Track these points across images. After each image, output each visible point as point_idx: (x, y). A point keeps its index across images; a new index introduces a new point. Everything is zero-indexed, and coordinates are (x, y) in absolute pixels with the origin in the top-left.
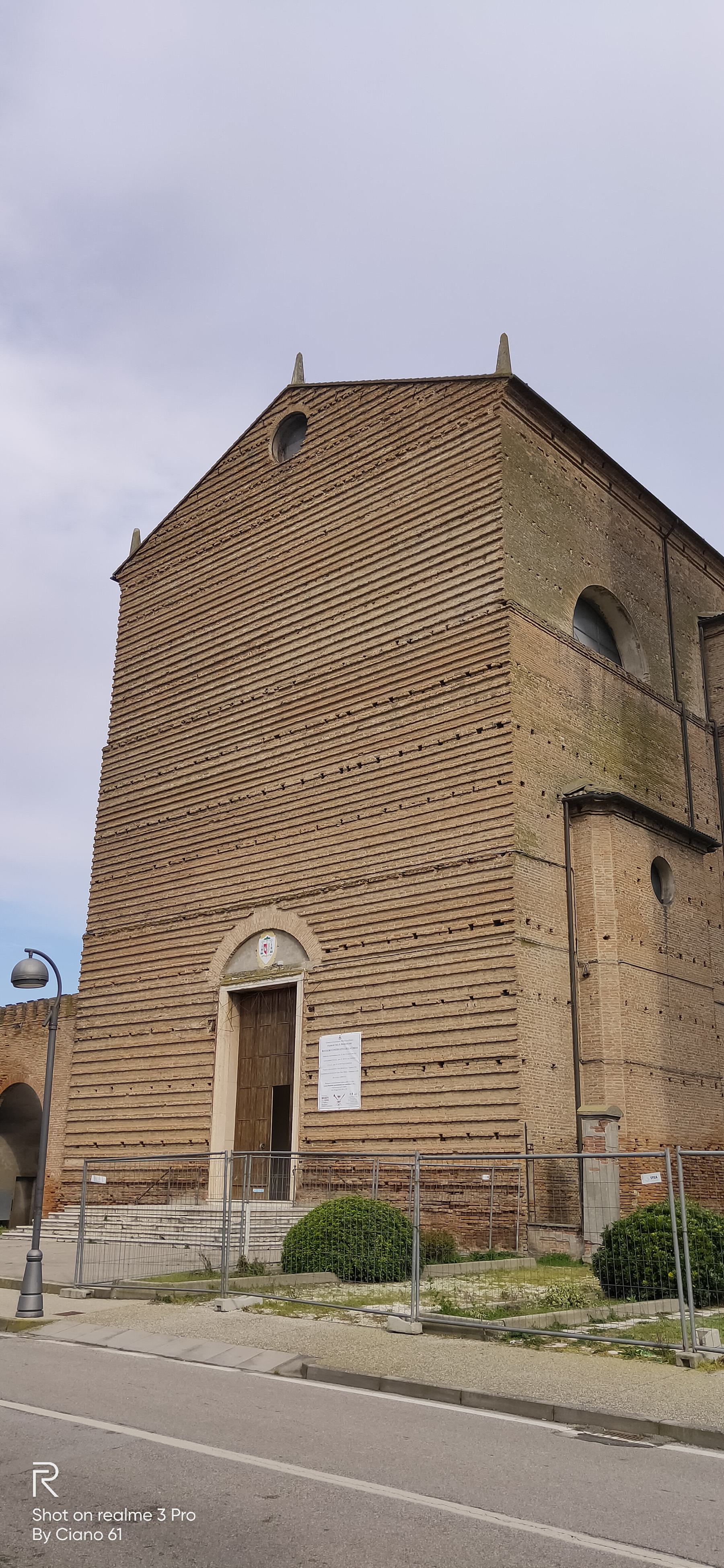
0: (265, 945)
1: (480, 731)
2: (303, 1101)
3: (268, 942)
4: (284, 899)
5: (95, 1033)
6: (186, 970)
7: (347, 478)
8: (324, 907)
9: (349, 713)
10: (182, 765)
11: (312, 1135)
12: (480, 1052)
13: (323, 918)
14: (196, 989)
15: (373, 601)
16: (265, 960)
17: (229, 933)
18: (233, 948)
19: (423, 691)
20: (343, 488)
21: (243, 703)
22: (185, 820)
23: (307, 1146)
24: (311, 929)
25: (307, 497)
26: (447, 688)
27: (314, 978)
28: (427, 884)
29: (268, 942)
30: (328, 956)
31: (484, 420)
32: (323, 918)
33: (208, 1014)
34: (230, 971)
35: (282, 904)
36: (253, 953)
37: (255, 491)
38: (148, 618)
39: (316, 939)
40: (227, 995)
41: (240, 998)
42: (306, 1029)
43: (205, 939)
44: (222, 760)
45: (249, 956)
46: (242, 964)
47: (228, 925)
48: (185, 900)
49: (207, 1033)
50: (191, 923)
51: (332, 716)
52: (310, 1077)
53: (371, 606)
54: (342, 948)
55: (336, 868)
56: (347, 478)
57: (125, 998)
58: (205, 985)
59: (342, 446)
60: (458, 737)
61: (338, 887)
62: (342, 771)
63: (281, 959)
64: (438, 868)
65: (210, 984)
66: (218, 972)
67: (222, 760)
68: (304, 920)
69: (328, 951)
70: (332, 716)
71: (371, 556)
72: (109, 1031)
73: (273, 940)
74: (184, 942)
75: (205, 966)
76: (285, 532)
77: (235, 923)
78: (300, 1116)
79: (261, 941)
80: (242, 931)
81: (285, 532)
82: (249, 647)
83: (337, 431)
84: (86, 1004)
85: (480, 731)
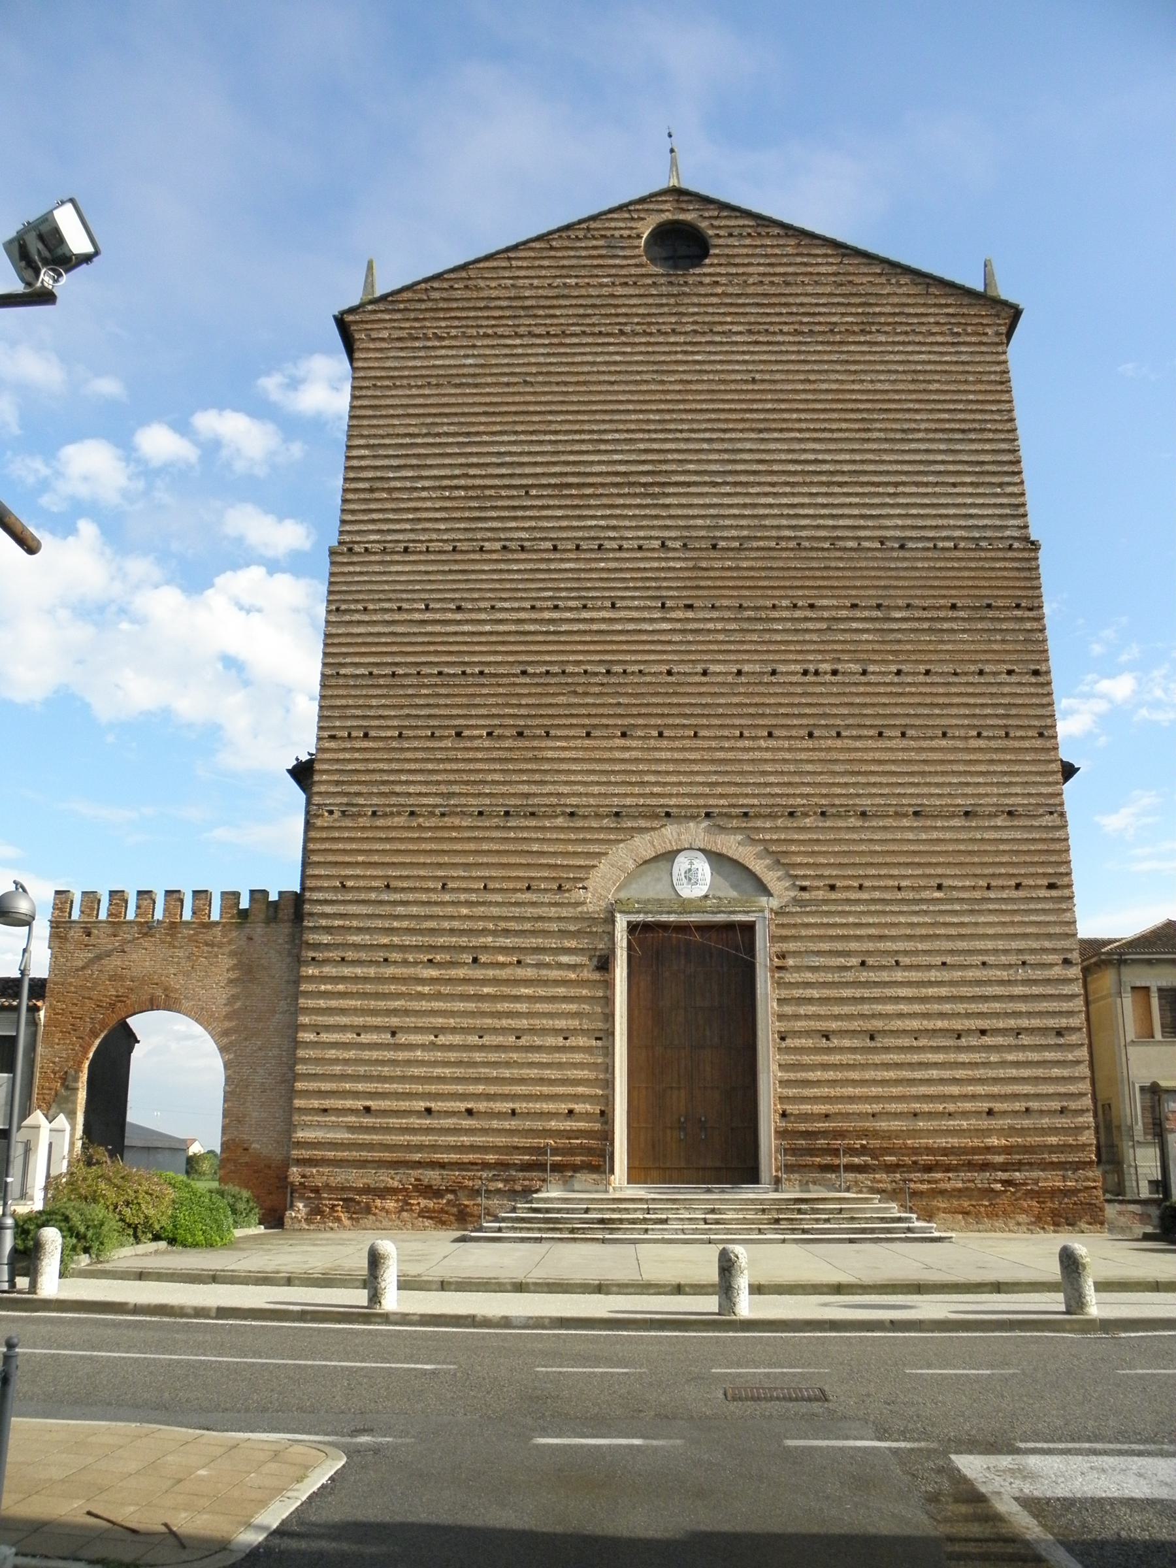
1: (1010, 672)
5: (350, 955)
7: (785, 328)
9: (812, 606)
10: (507, 605)
11: (790, 1108)
12: (1036, 1022)
15: (840, 484)
19: (924, 609)
20: (780, 338)
21: (620, 548)
22: (517, 680)
25: (719, 328)
26: (955, 614)
28: (951, 831)
30: (806, 895)
31: (984, 339)
37: (620, 291)
38: (414, 391)
40: (625, 925)
44: (585, 615)
46: (649, 888)
48: (525, 789)
51: (785, 603)
53: (837, 490)
55: (808, 790)
56: (785, 328)
57: (414, 910)
59: (773, 290)
60: (981, 673)
62: (805, 673)
64: (967, 814)
67: (585, 615)
69: (803, 889)
70: (785, 603)
71: (831, 431)
72: (379, 956)
76: (680, 357)
80: (644, 846)
81: (680, 357)
82: (627, 481)
83: (762, 269)
84: (328, 909)
85: (1010, 672)
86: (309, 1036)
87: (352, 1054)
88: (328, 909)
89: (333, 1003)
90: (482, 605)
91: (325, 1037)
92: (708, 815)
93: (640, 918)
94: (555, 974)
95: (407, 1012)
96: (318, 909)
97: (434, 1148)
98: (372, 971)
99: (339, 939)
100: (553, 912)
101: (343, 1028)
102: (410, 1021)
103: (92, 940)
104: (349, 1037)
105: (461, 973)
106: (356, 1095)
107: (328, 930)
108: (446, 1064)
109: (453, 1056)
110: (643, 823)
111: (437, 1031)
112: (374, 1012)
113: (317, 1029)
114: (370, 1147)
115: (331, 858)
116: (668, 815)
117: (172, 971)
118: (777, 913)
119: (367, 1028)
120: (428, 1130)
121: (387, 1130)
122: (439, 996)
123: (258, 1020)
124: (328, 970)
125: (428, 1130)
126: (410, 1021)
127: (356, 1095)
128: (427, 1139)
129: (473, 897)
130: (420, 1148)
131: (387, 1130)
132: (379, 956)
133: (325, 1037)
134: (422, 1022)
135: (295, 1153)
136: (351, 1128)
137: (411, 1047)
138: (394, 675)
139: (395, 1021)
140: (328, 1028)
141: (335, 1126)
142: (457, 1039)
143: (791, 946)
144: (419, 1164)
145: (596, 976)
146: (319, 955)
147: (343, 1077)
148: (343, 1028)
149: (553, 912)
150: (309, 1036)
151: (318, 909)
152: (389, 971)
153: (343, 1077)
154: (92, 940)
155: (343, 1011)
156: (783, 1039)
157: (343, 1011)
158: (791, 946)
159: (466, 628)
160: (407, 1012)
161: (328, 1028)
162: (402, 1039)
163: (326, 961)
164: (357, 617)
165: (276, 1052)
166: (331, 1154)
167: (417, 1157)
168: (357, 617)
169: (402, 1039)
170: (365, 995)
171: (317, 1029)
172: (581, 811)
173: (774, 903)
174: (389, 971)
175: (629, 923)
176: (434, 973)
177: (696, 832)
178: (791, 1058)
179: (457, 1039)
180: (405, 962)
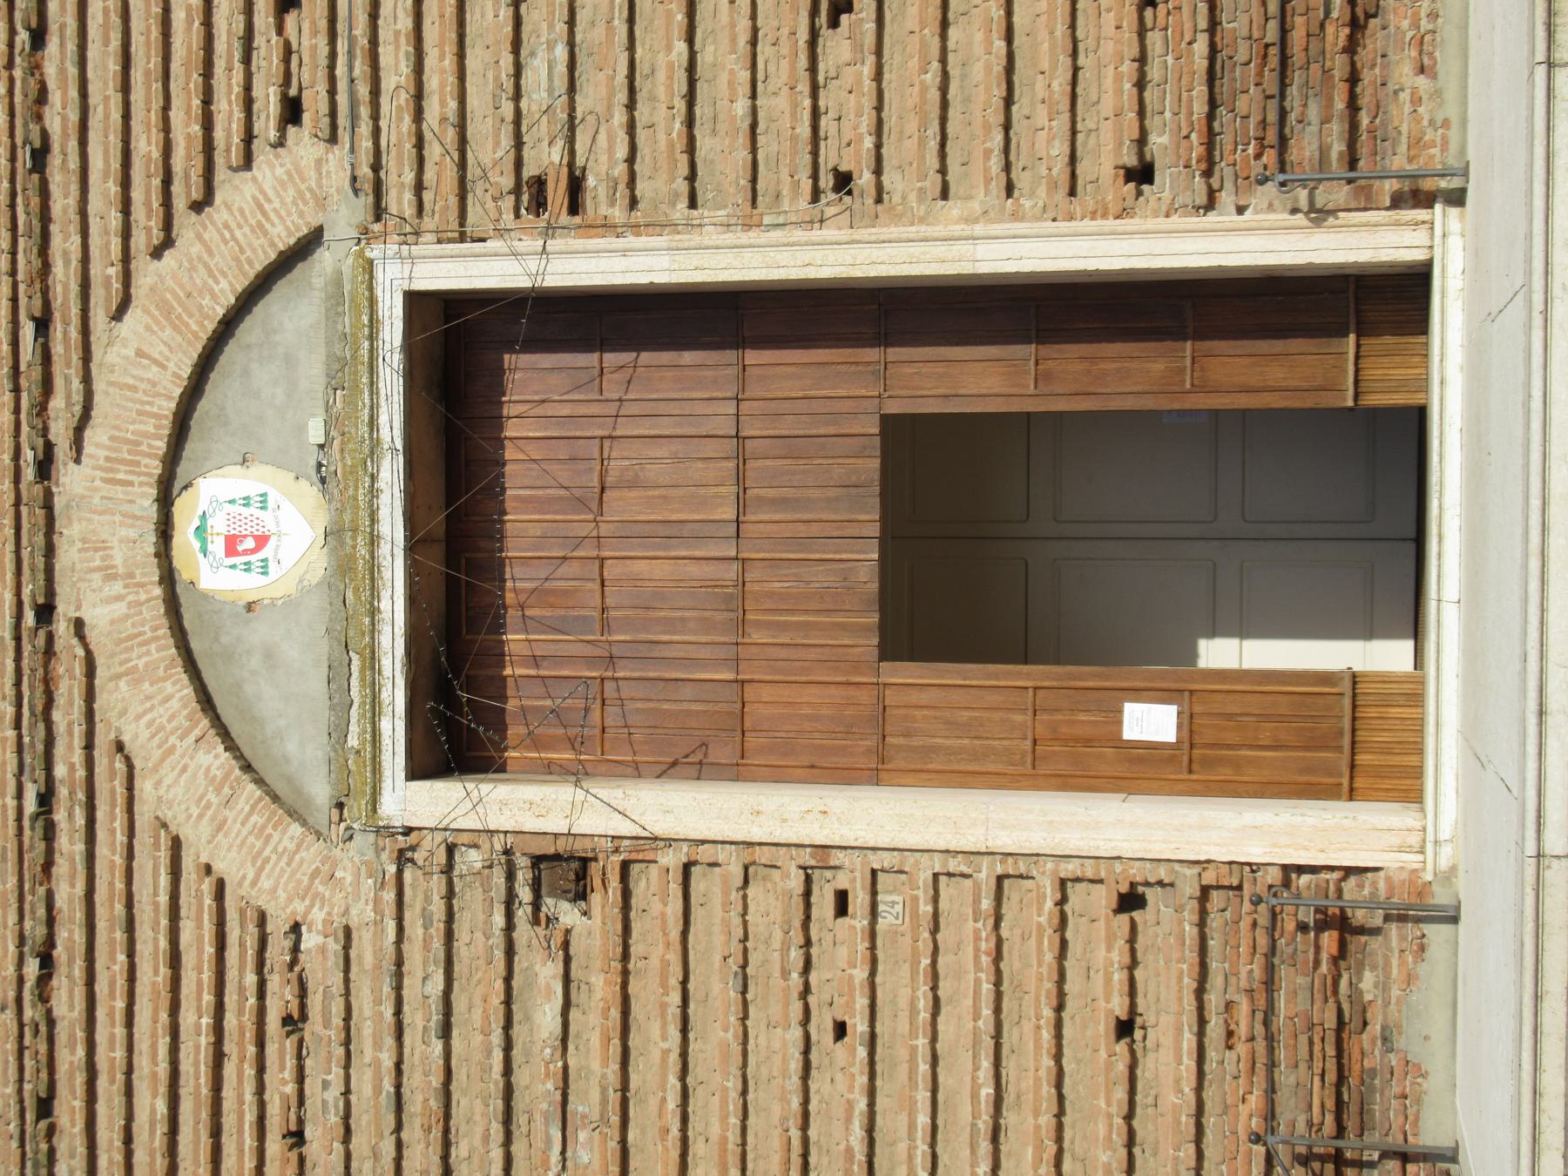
0: (231, 550)
2: (954, 208)
3: (219, 526)
4: (42, 408)
6: (280, 1083)
8: (103, 159)
11: (1106, 154)
13: (146, 146)
14: (372, 1008)
16: (296, 530)
17: (145, 787)
18: (216, 758)
23: (1164, 176)
24: (184, 220)
27: (399, 200)
29: (219, 526)
30: (315, 104)
32: (146, 146)
33: (499, 920)
34: (320, 792)
35: (60, 432)
36: (259, 632)
39: (234, 191)
41: (457, 727)
42: (618, 214)
43: (152, 941)
45: (269, 655)
47: (109, 787)
49: (588, 924)
50: (70, 1058)
52: (843, 181)
54: (290, 19)
58: (366, 952)
61: (35, 68)
63: (302, 429)
65: (361, 914)
66: (313, 852)
68: (147, 274)
69: (292, 111)
73: (213, 495)
74: (151, 1105)
75: (278, 952)
77: (103, 740)
78: (1016, 216)
79: (211, 574)
80: (144, 705)
92: (45, 467)
93: (394, 730)
94: (593, 1062)
100: (374, 1053)
110: (67, 715)
116: (46, 612)
118: (379, 212)
143: (490, 148)
145: (604, 901)
149: (374, 1053)
156: (843, 181)
158: (490, 148)
172: (35, 930)
173: (344, 217)
175: (418, 770)
177: (100, 504)
178: (909, 146)
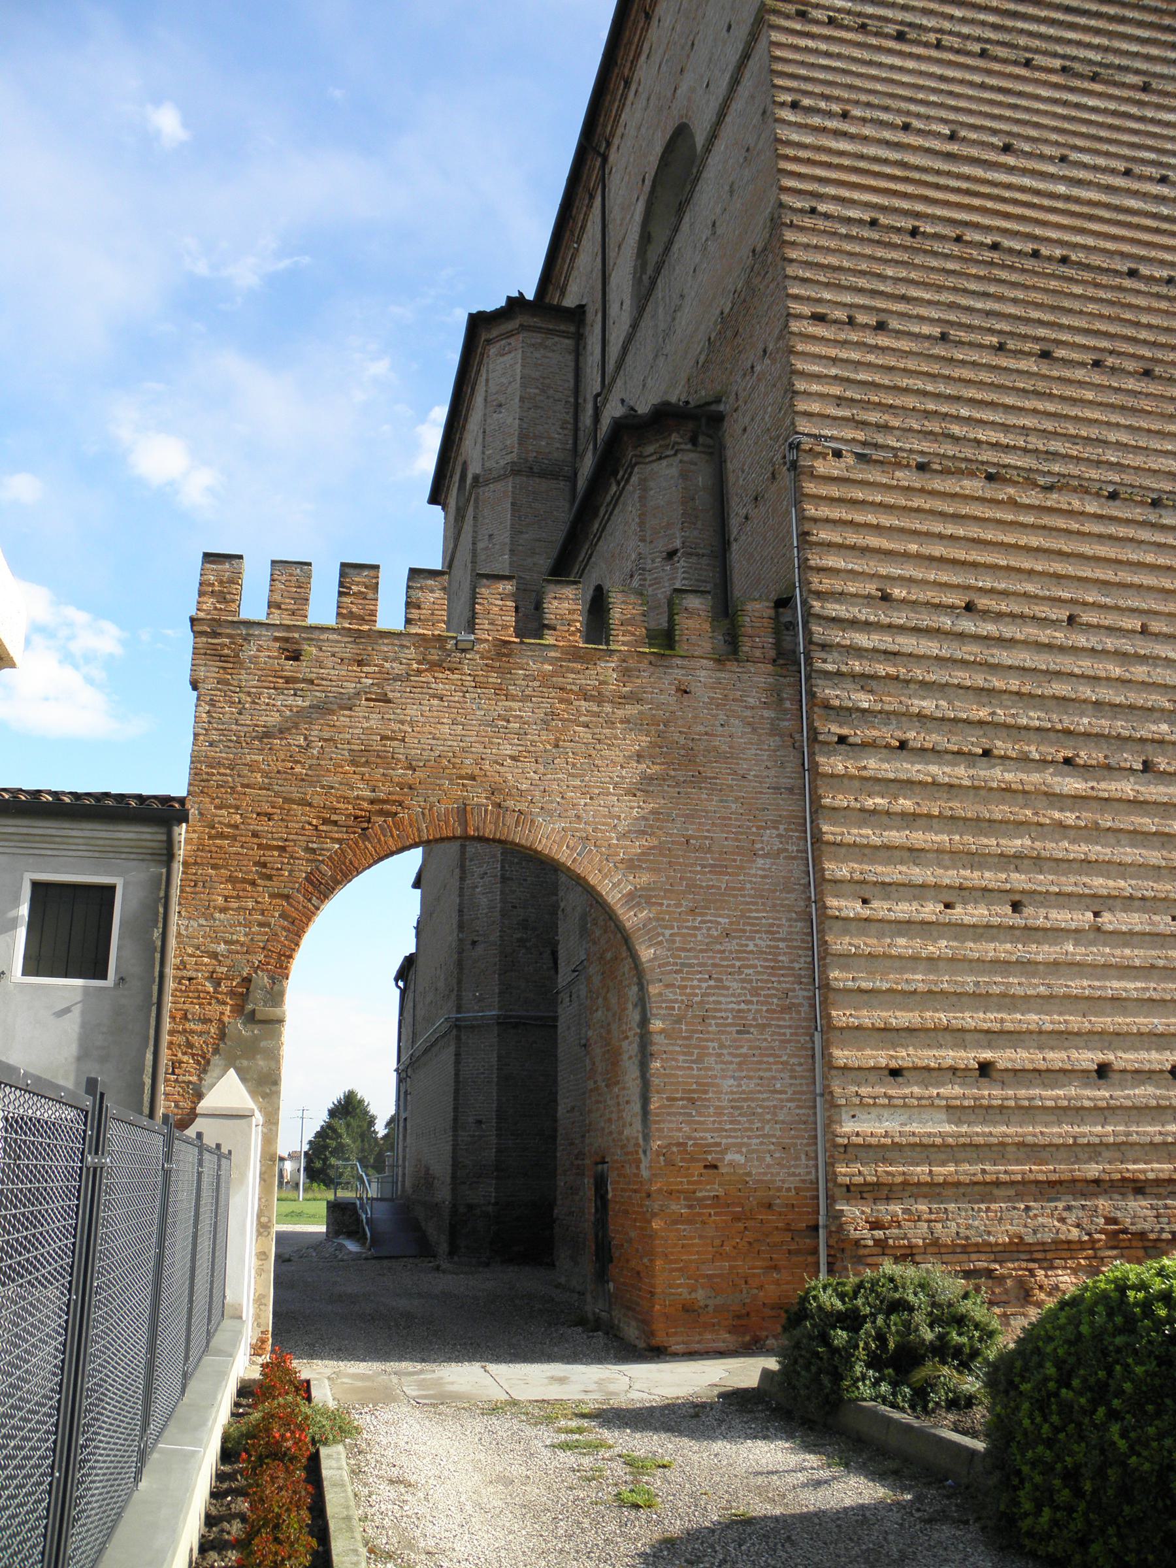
84: (863, 640)
86: (852, 908)
87: (941, 947)
88: (863, 640)
89: (895, 836)
90: (1048, 150)
91: (880, 908)
95: (1038, 862)
96: (837, 636)
97: (1122, 1149)
98: (961, 773)
99: (891, 703)
101: (919, 891)
102: (1044, 881)
103: (303, 669)
104: (930, 910)
105: (1126, 788)
106: (958, 1036)
107: (865, 681)
108: (1126, 970)
109: (1136, 955)
111: (1099, 903)
112: (976, 860)
113: (865, 891)
114: (998, 1150)
115: (853, 538)
117: (508, 750)
119: (965, 893)
120: (1104, 1112)
121: (1028, 1112)
122: (1094, 833)
123: (718, 869)
124: (874, 765)
125: (1104, 1112)
126: (1044, 881)
127: (958, 1036)
128: (1109, 1131)
129: (1125, 645)
130: (1095, 1150)
131: (1028, 1112)
132: (973, 743)
133: (880, 908)
134: (1069, 883)
135: (845, 1171)
136: (955, 1111)
137: (1056, 934)
138: (914, 232)
139: (1019, 880)
140: (887, 889)
141: (927, 1105)
142: (1135, 921)
144: (1097, 1186)
146: (858, 734)
147: (933, 997)
148: (919, 891)
150: (852, 908)
151: (837, 636)
152: (999, 775)
153: (933, 997)
154: (303, 669)
155: (914, 854)
157: (914, 854)
159: (1027, 182)
160: (1038, 862)
161: (887, 889)
162: (1035, 916)
163: (868, 746)
164: (831, 124)
165: (763, 942)
166: (920, 1171)
167: (1093, 1170)
168: (831, 124)
169: (1035, 916)
170: (952, 821)
171: (865, 891)
174: (999, 775)
176: (1073, 785)
179: (1135, 921)
180: (1024, 760)
